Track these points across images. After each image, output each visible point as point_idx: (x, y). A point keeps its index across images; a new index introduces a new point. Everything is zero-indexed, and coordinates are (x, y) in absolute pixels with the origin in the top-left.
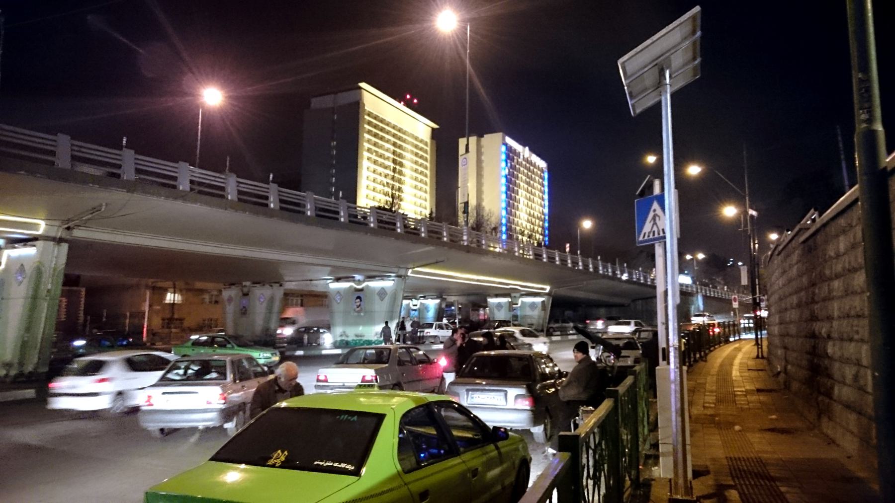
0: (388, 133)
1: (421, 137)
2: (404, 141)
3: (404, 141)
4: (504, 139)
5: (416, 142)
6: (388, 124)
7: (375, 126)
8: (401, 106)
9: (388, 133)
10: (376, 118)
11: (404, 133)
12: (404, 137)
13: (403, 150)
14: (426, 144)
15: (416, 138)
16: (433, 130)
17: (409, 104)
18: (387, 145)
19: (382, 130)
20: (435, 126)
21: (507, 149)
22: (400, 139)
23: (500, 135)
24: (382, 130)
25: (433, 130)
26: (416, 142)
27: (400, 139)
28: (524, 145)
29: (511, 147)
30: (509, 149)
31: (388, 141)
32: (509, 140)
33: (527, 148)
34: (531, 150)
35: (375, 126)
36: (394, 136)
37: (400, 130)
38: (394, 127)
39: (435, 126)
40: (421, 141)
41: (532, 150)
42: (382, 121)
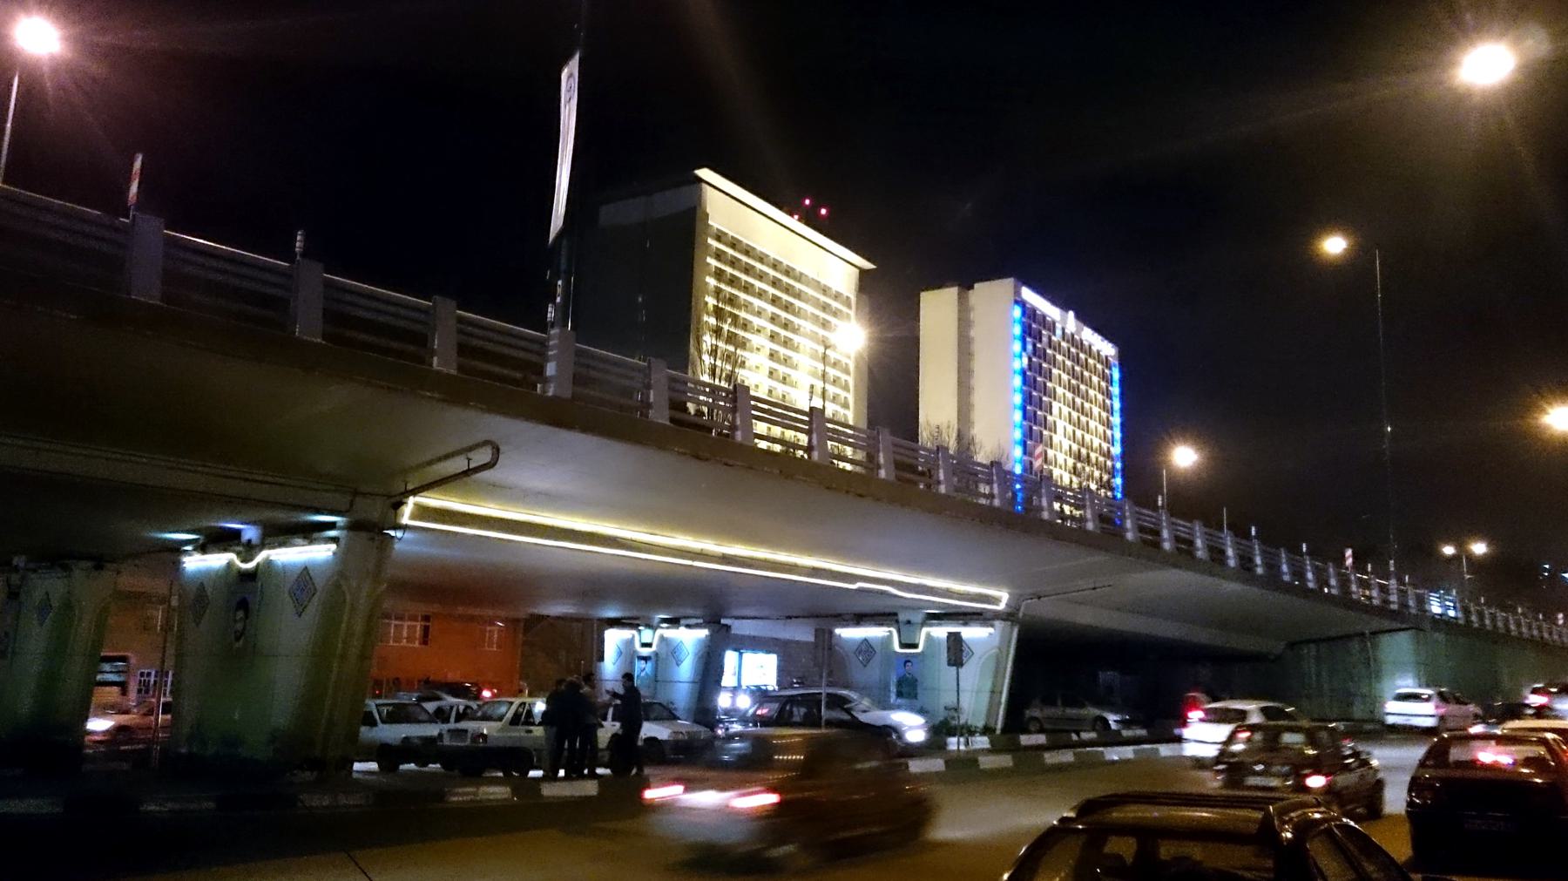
0: (761, 276)
1: (836, 286)
2: (798, 295)
3: (798, 295)
4: (1017, 293)
5: (823, 298)
6: (762, 258)
7: (733, 263)
8: (793, 222)
9: (761, 276)
10: (734, 244)
11: (799, 278)
12: (798, 285)
13: (794, 313)
14: (847, 302)
15: (825, 290)
16: (863, 273)
17: (810, 220)
18: (757, 302)
19: (748, 270)
20: (868, 265)
21: (1024, 313)
22: (788, 290)
23: (1009, 283)
24: (748, 270)
25: (863, 273)
26: (823, 298)
27: (788, 290)
28: (1064, 306)
29: (1034, 310)
30: (1030, 314)
31: (761, 295)
32: (1028, 294)
33: (1071, 314)
34: (1078, 317)
35: (733, 263)
36: (775, 283)
37: (788, 272)
38: (775, 265)
39: (868, 265)
40: (837, 296)
41: (1083, 318)
42: (748, 251)
